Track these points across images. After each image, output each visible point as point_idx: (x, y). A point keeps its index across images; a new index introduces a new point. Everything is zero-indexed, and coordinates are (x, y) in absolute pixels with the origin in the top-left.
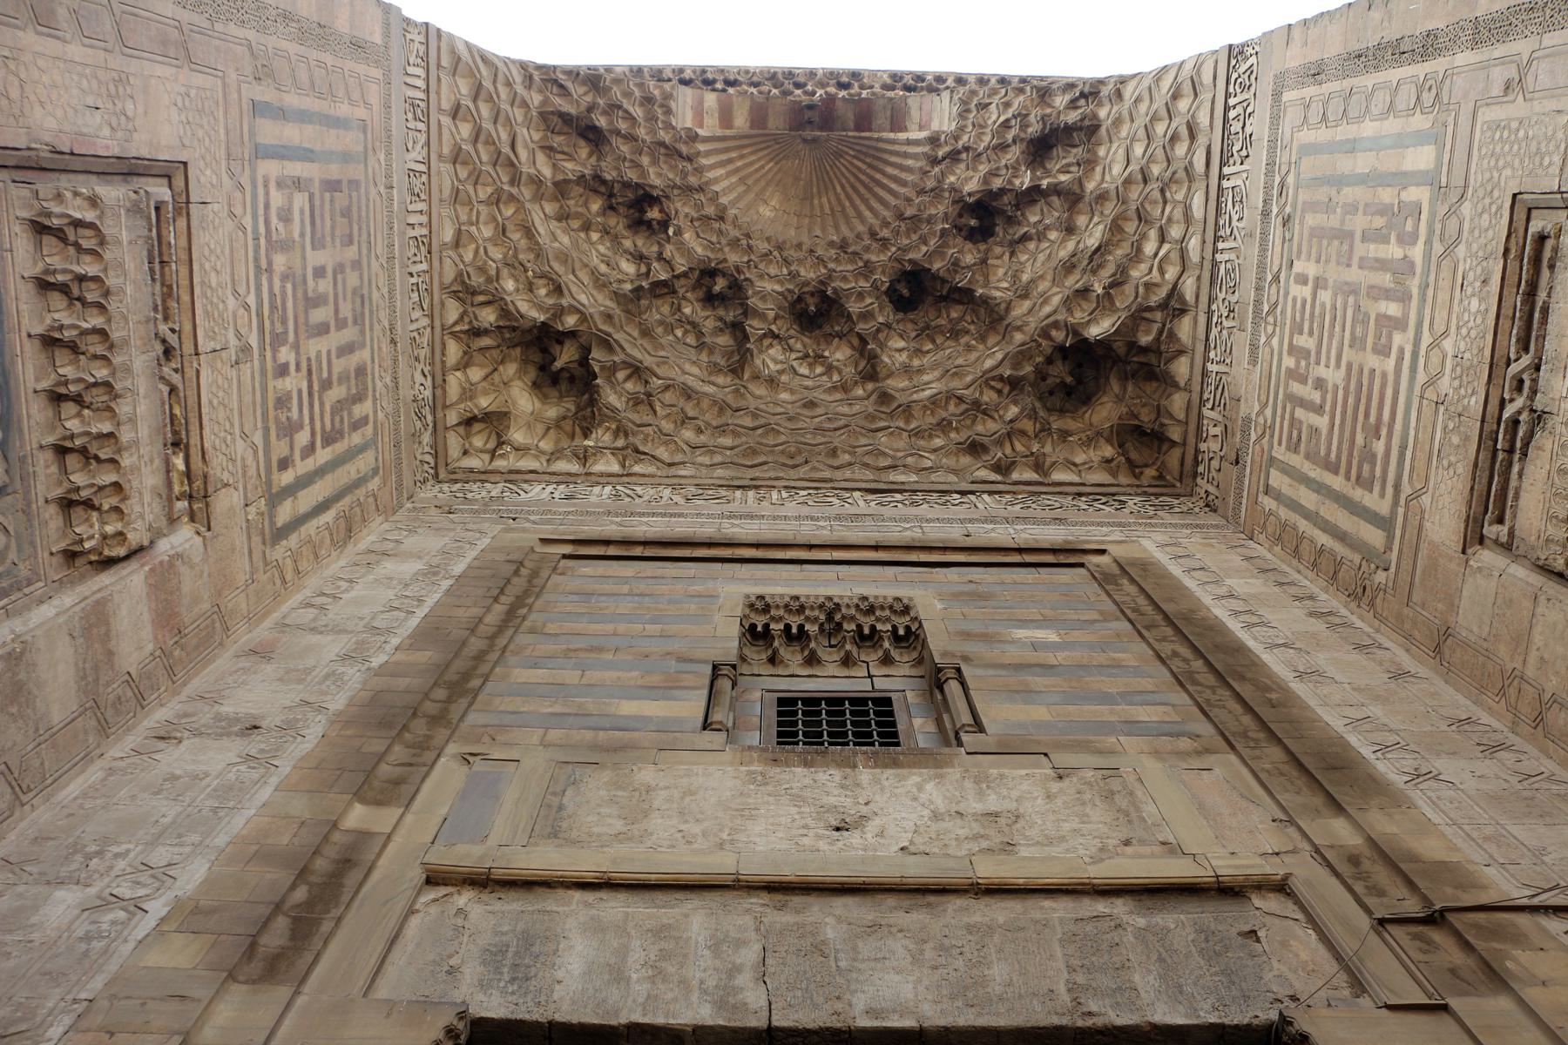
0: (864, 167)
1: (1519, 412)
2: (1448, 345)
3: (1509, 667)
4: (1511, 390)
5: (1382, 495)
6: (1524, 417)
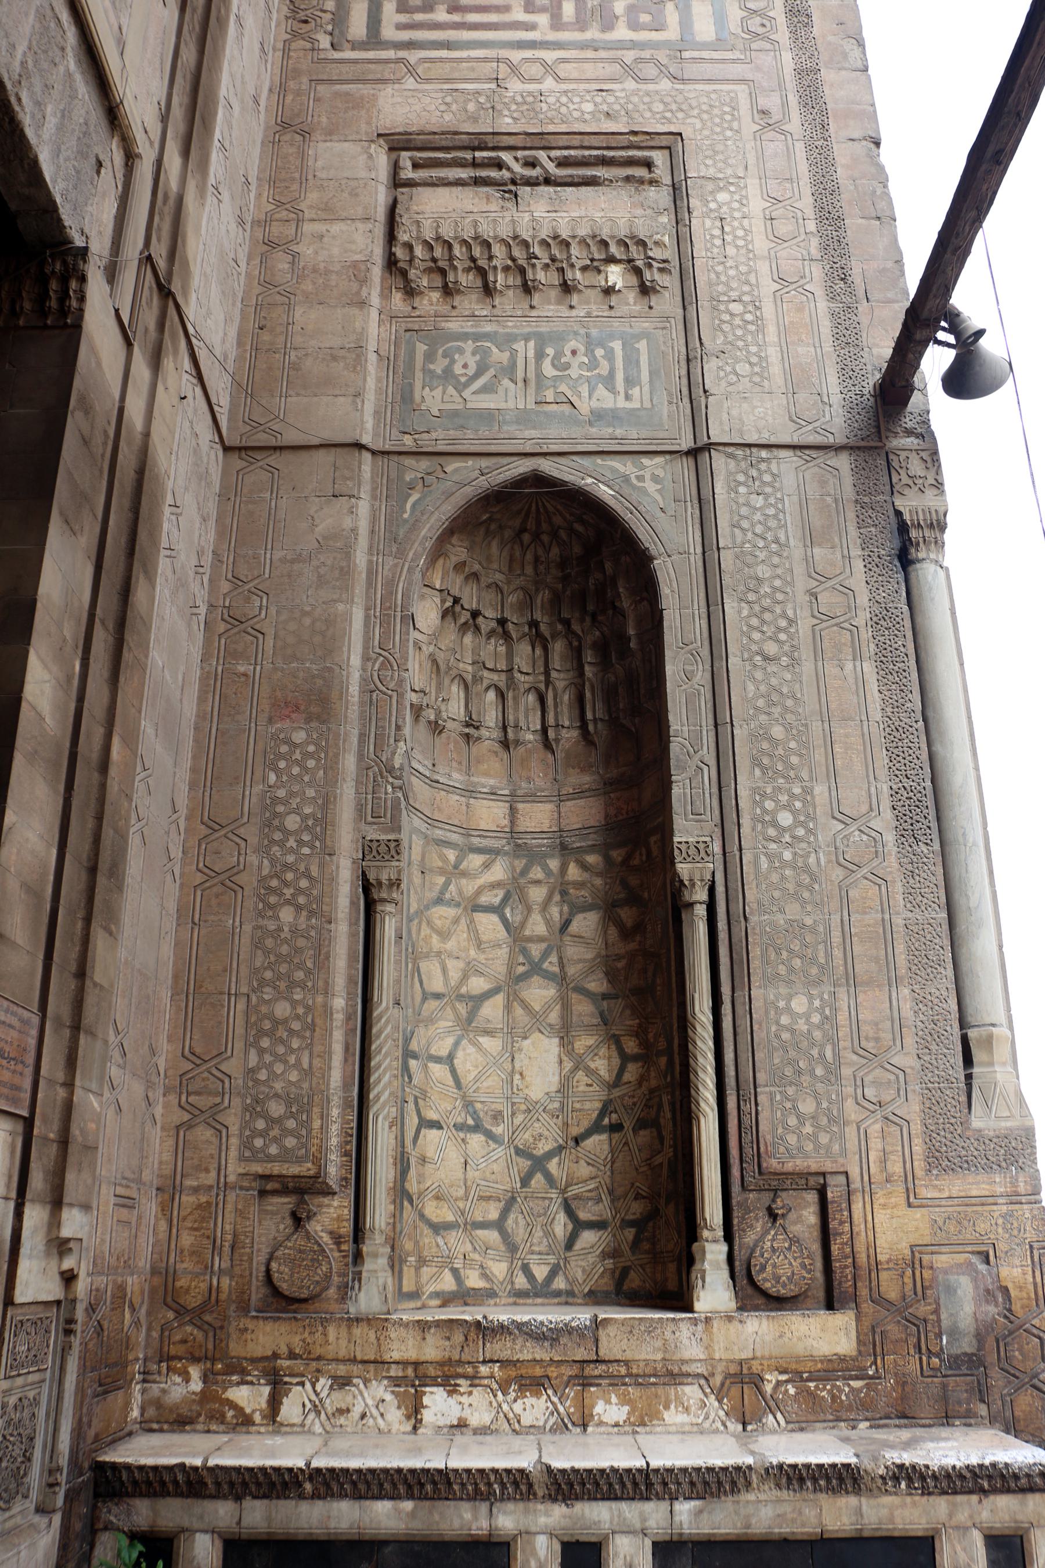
1: (509, 169)
2: (549, 83)
3: (303, 206)
4: (525, 157)
5: (400, 27)
6: (506, 174)
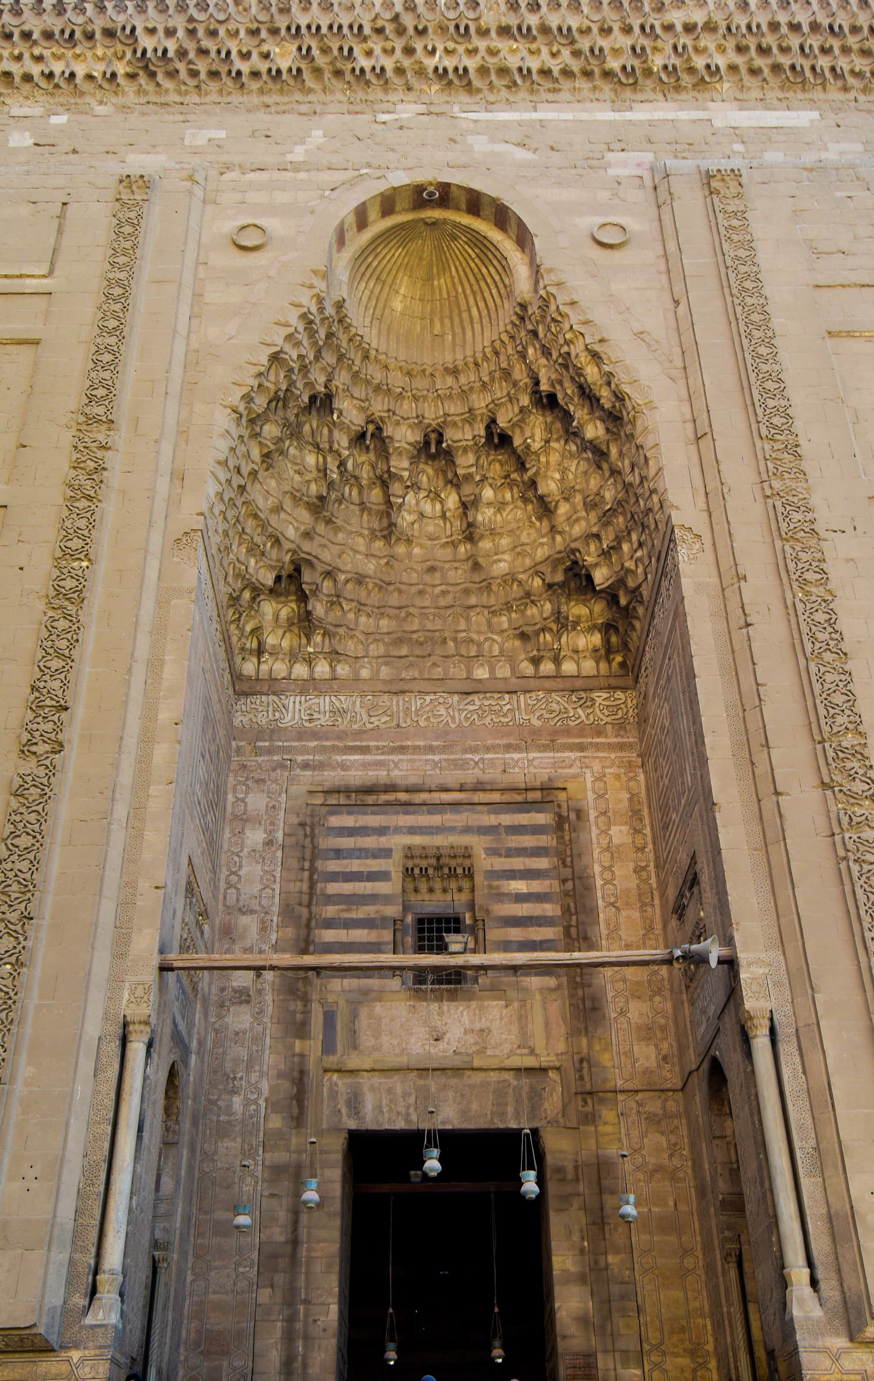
0: (473, 256)
